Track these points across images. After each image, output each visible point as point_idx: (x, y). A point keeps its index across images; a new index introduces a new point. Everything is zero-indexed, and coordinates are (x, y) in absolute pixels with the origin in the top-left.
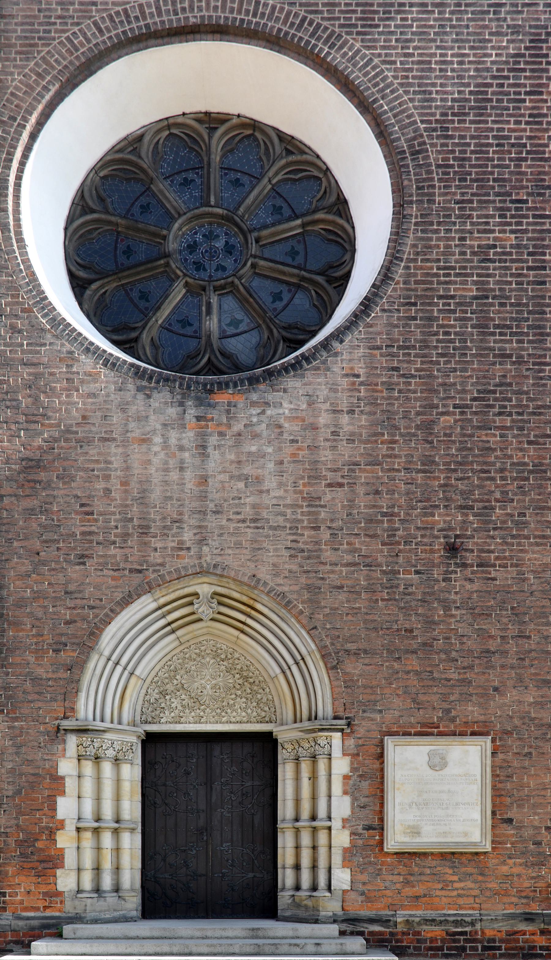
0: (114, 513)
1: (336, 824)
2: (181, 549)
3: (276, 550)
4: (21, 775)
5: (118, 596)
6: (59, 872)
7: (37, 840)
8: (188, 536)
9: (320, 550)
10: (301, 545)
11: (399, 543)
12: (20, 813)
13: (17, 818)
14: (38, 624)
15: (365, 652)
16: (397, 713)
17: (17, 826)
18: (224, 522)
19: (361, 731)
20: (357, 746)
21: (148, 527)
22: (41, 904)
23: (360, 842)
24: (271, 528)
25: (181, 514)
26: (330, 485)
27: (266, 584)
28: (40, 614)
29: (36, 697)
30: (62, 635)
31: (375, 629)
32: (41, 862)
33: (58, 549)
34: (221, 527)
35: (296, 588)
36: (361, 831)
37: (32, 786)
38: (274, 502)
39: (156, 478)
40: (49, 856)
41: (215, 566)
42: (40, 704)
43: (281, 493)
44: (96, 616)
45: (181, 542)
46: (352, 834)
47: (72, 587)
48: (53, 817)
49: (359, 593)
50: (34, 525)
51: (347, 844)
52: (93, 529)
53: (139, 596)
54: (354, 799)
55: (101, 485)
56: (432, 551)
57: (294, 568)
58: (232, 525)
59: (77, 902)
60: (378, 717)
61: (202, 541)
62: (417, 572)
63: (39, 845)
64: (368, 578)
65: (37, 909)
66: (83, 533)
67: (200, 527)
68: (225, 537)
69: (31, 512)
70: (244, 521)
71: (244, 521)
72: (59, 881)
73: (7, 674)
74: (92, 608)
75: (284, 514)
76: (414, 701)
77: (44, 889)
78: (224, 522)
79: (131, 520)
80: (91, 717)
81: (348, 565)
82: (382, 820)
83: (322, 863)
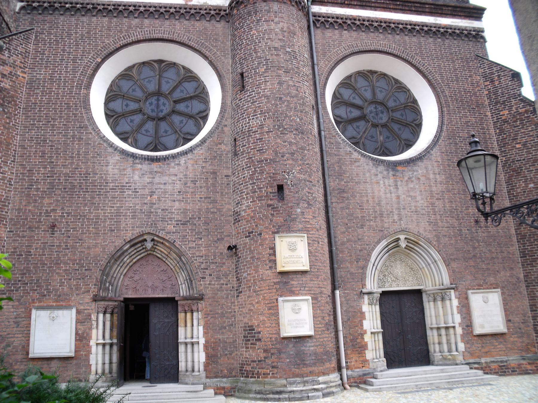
0: (371, 209)
1: (457, 325)
2: (394, 222)
3: (424, 222)
4: (349, 312)
5: (376, 240)
6: (366, 351)
7: (357, 339)
8: (396, 217)
9: (437, 222)
10: (432, 221)
11: (460, 220)
12: (350, 328)
13: (349, 330)
14: (350, 251)
15: (457, 259)
16: (470, 282)
17: (350, 333)
18: (407, 213)
19: (460, 288)
20: (459, 295)
21: (383, 214)
22: (361, 365)
23: (465, 332)
24: (421, 214)
25: (392, 209)
26: (437, 199)
27: (422, 235)
28: (350, 248)
29: (352, 280)
30: (359, 255)
31: (458, 251)
32: (359, 348)
33: (354, 223)
34: (406, 214)
35: (432, 236)
36: (465, 327)
37: (354, 317)
38: (421, 205)
39: (383, 196)
40: (363, 345)
41: (406, 228)
42: (353, 283)
43: (422, 202)
44: (369, 248)
45: (394, 220)
46: (463, 329)
47: (360, 237)
48: (362, 329)
49: (452, 238)
50: (345, 213)
51: (461, 333)
52: (365, 215)
53: (383, 240)
54: (461, 315)
55: (365, 199)
56: (471, 222)
57: (431, 229)
58: (409, 213)
59: (374, 364)
60: (464, 283)
61: (401, 219)
62: (468, 230)
63: (358, 341)
64: (453, 232)
65: (359, 368)
66: (361, 217)
67: (399, 214)
68: (408, 218)
69: (342, 208)
70: (413, 212)
71: (413, 212)
72: (367, 355)
73: (341, 272)
74: (367, 245)
75: (424, 209)
76: (474, 276)
77: (361, 359)
78: (407, 213)
79: (377, 212)
80: (373, 288)
81: (447, 227)
82: (471, 323)
83: (453, 341)
